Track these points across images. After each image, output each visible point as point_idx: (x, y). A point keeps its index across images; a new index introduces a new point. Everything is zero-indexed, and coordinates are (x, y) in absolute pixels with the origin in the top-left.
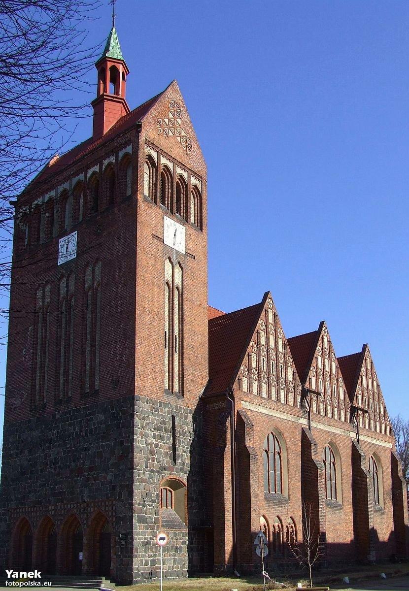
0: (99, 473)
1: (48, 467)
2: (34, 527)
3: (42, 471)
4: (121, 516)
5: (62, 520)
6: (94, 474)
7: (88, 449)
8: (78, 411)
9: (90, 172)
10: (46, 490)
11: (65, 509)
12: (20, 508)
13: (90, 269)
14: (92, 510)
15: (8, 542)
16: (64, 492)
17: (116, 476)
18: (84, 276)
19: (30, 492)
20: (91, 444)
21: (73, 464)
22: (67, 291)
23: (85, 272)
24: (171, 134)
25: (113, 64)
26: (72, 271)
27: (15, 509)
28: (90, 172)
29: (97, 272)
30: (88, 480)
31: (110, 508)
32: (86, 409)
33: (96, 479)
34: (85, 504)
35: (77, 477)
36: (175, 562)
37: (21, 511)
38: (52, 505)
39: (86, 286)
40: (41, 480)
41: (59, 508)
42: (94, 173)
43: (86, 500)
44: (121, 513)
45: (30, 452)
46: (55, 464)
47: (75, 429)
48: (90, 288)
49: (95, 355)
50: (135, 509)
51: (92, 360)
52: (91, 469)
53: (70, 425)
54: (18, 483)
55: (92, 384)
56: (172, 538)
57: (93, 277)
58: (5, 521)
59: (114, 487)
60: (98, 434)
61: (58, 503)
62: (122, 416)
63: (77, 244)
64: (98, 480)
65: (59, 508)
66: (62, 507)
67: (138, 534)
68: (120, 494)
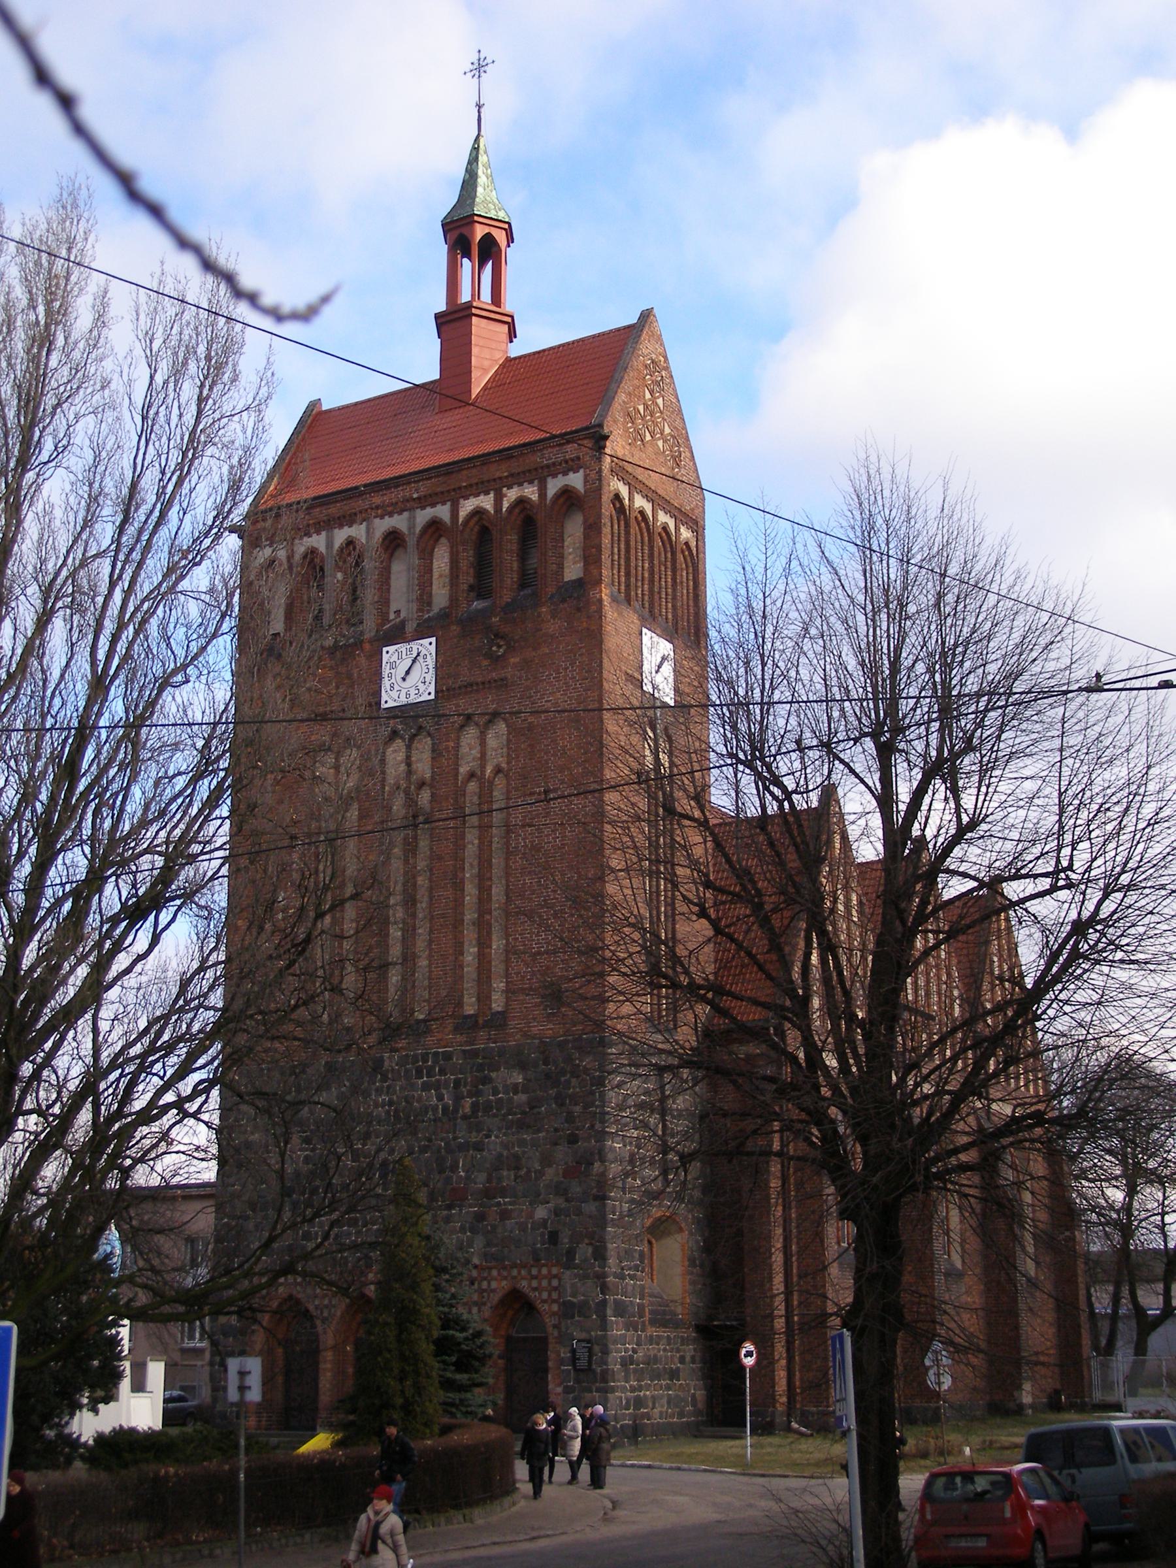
0: (510, 1203)
4: (575, 1300)
7: (479, 1147)
8: (448, 1056)
9: (468, 506)
10: (359, 1233)
13: (471, 733)
14: (494, 1285)
17: (557, 1212)
18: (457, 747)
20: (488, 1136)
22: (409, 773)
23: (458, 738)
24: (648, 437)
25: (487, 230)
26: (420, 728)
28: (468, 506)
29: (492, 742)
30: (480, 1217)
31: (545, 1283)
32: (474, 1054)
33: (505, 1215)
36: (669, 1403)
39: (462, 770)
42: (478, 512)
44: (574, 1296)
47: (440, 1098)
48: (472, 775)
49: (489, 934)
50: (610, 1286)
51: (483, 943)
52: (487, 1194)
53: (426, 1087)
55: (484, 998)
56: (665, 1350)
57: (483, 755)
59: (554, 1238)
60: (505, 1115)
62: (574, 1080)
63: (436, 668)
64: (509, 1218)
67: (615, 1342)
68: (571, 1253)
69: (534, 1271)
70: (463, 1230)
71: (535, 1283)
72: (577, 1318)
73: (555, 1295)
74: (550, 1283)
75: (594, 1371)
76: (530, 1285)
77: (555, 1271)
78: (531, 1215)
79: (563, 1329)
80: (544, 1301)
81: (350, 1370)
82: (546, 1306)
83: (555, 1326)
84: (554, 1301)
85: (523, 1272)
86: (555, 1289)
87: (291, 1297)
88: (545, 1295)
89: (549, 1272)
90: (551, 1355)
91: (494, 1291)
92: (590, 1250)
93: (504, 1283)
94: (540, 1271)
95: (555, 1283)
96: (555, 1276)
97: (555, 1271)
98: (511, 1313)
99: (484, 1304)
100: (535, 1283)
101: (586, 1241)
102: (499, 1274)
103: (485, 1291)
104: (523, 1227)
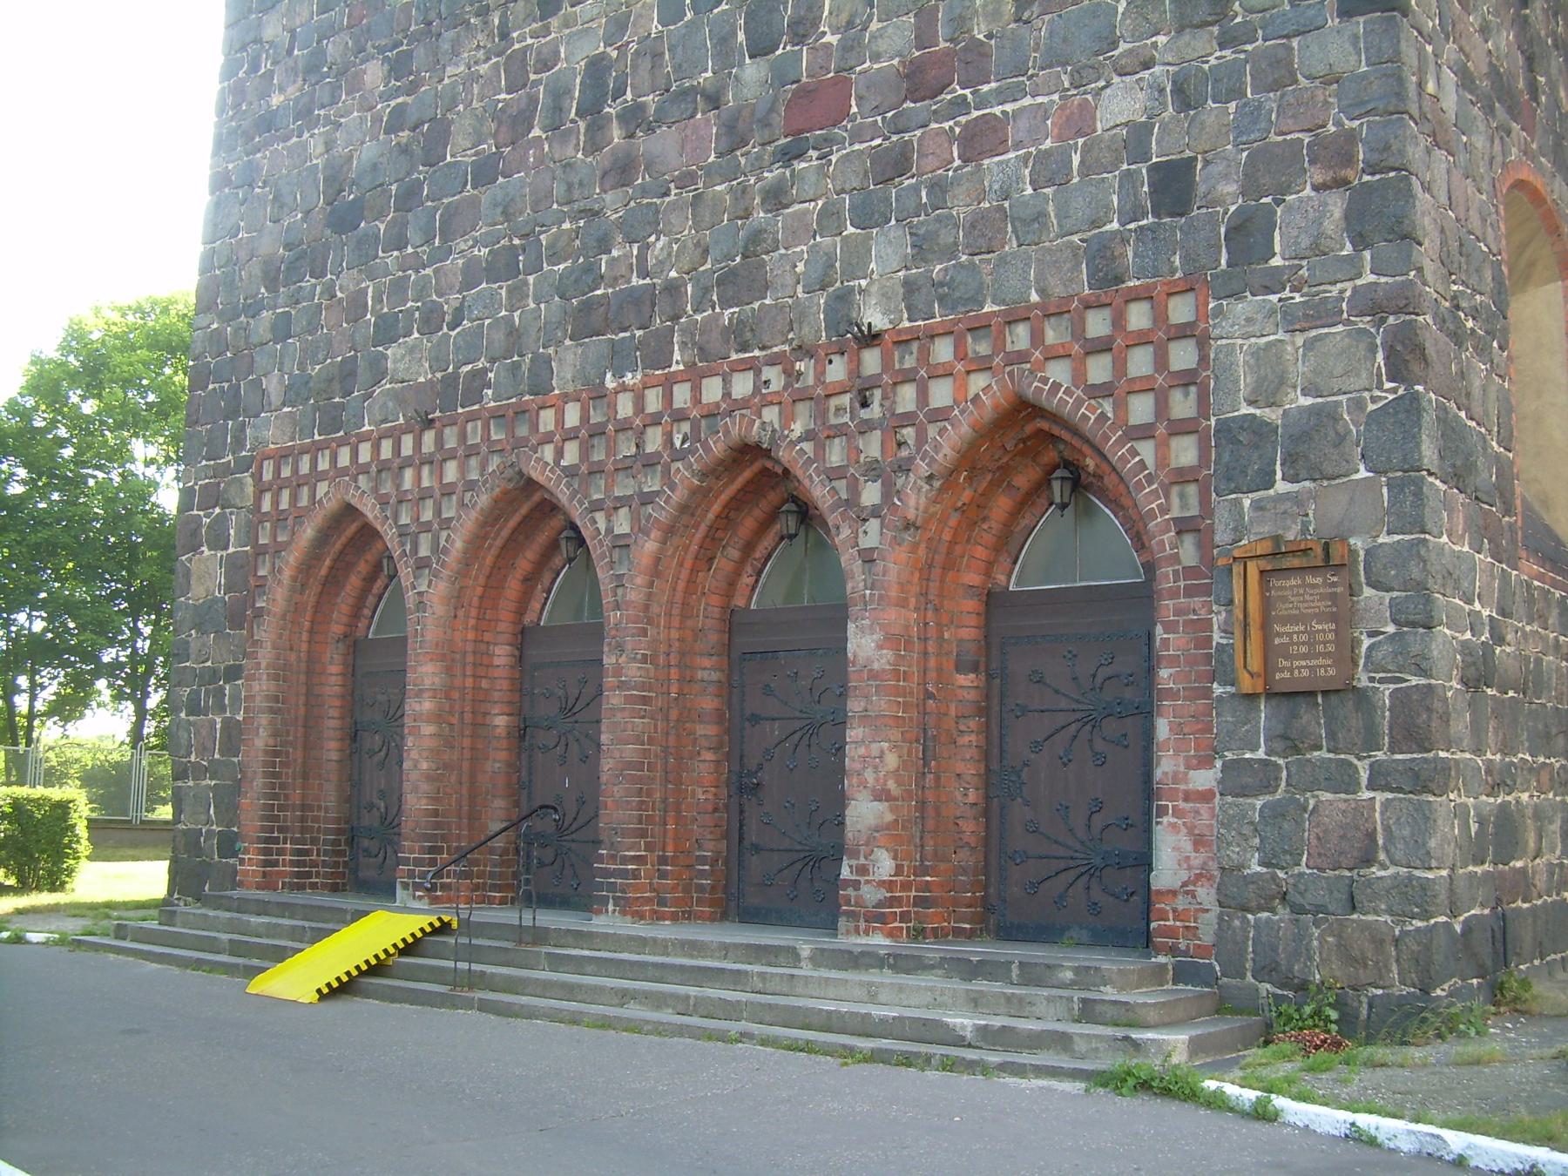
0: (1002, 96)
1: (536, 132)
2: (423, 564)
3: (485, 172)
4: (1272, 415)
5: (647, 499)
6: (961, 105)
10: (517, 294)
11: (680, 416)
12: (316, 448)
14: (941, 393)
15: (233, 673)
16: (673, 289)
17: (1185, 95)
19: (388, 331)
21: (752, 71)
27: (281, 456)
30: (895, 164)
34: (871, 360)
35: (788, 156)
37: (324, 464)
38: (566, 398)
40: (482, 230)
41: (625, 407)
43: (875, 317)
45: (399, 68)
46: (591, 110)
54: (309, 281)
58: (219, 542)
61: (619, 374)
64: (1000, 147)
65: (625, 407)
66: (653, 402)
69: (1097, 324)
70: (830, 219)
71: (1099, 370)
72: (1281, 486)
73: (1183, 405)
74: (1161, 361)
75: (1363, 698)
76: (1079, 376)
77: (1181, 310)
78: (1079, 122)
79: (1222, 536)
80: (1144, 432)
81: (501, 721)
82: (1146, 450)
83: (1183, 527)
84: (1181, 428)
85: (1053, 335)
86: (1187, 379)
87: (349, 511)
88: (1141, 409)
89: (1160, 316)
90: (1170, 640)
91: (940, 415)
92: (1337, 205)
93: (978, 382)
94: (1119, 321)
95: (1183, 356)
96: (1183, 332)
97: (1181, 310)
98: (1002, 505)
99: (904, 467)
100: (1099, 370)
101: (1317, 175)
102: (960, 354)
103: (908, 419)
104: (1050, 171)
